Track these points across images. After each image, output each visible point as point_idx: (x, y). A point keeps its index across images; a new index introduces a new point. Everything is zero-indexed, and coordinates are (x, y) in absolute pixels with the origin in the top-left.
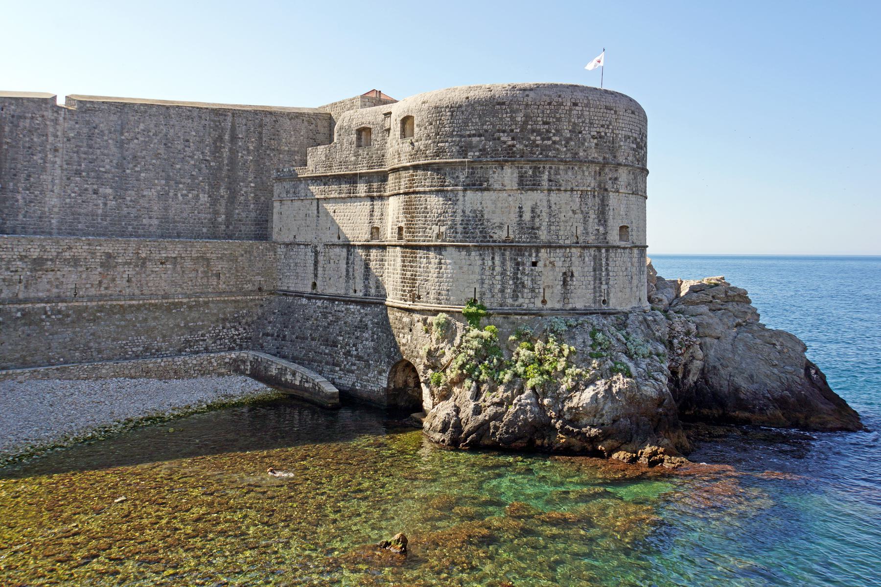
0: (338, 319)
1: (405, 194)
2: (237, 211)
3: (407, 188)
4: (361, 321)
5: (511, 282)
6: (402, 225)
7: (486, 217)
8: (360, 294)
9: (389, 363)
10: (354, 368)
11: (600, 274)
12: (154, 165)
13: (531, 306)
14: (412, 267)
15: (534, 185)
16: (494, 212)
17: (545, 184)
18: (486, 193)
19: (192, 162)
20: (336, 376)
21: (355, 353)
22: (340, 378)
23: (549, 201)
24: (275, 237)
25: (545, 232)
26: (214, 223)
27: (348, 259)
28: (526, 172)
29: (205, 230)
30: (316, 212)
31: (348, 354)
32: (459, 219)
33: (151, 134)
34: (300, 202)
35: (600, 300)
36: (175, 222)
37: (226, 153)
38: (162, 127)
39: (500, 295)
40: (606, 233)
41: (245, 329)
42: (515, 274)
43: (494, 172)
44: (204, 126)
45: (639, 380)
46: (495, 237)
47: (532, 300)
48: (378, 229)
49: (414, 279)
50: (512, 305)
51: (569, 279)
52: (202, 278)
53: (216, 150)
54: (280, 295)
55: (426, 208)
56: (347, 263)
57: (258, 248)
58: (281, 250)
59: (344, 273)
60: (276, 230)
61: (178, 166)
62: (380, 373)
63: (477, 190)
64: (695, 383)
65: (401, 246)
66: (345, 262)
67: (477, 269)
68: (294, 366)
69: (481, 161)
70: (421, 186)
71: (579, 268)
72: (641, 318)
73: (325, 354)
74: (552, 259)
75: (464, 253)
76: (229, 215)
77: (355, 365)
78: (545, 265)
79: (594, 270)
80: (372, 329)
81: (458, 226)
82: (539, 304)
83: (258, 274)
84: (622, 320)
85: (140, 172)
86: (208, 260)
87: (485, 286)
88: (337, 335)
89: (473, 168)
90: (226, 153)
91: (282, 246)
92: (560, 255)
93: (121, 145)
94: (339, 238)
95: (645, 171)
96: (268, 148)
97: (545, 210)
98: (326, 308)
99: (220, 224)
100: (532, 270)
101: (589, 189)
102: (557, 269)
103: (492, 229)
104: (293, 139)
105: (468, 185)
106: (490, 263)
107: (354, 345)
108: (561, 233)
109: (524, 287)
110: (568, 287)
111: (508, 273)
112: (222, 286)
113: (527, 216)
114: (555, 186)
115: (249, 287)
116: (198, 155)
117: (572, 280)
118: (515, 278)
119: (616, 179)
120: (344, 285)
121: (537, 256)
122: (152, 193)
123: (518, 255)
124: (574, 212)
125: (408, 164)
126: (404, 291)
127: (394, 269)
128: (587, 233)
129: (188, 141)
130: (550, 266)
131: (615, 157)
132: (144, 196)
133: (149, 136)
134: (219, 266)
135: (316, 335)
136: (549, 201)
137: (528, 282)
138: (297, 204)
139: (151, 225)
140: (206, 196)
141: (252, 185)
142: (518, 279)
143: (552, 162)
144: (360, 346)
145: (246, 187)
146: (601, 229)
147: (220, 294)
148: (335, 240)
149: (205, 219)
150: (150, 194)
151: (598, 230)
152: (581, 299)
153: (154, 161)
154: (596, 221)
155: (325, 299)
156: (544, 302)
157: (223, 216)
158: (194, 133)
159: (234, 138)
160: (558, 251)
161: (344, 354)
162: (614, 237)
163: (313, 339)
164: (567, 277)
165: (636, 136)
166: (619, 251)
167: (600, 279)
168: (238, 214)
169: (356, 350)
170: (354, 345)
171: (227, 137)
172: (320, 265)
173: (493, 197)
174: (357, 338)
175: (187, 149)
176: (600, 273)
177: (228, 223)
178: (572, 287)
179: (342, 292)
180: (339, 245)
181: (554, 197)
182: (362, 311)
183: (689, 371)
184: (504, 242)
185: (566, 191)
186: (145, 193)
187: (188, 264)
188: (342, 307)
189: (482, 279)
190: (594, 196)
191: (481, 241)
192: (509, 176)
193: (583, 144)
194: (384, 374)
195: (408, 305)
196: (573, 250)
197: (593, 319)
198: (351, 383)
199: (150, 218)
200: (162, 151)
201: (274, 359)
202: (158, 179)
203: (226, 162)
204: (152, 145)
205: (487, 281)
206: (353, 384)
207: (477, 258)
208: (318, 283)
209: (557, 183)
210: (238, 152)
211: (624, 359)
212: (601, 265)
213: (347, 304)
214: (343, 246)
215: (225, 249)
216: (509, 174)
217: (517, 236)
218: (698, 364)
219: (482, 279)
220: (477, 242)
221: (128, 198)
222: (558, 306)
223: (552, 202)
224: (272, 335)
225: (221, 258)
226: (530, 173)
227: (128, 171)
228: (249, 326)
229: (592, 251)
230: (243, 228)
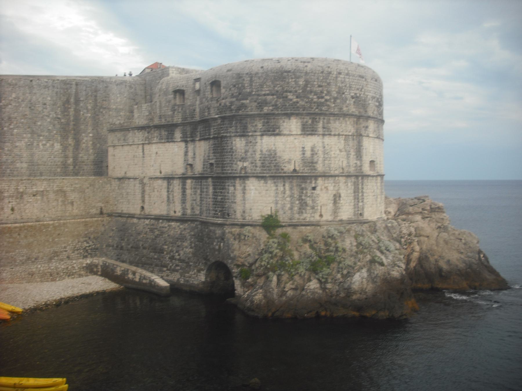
0: (162, 233)
1: (214, 138)
2: (81, 155)
3: (215, 134)
4: (181, 234)
5: (297, 202)
6: (212, 161)
7: (278, 155)
8: (179, 214)
9: (206, 263)
10: (178, 268)
11: (358, 195)
12: (22, 123)
13: (312, 219)
14: (221, 192)
15: (313, 131)
16: (284, 151)
17: (320, 130)
18: (278, 137)
19: (49, 120)
20: (164, 274)
21: (178, 257)
22: (168, 276)
23: (323, 142)
24: (110, 173)
25: (321, 165)
26: (65, 165)
27: (168, 188)
28: (307, 122)
29: (59, 170)
30: (141, 154)
31: (172, 258)
32: (258, 156)
33: (20, 100)
34: (128, 147)
35: (358, 213)
36: (38, 165)
37: (72, 111)
38: (27, 95)
39: (289, 212)
40: (361, 166)
41: (93, 242)
42: (300, 196)
43: (284, 122)
44: (57, 93)
45: (389, 267)
46: (286, 169)
47: (313, 215)
48: (191, 165)
49: (223, 202)
50: (298, 219)
51: (337, 199)
52: (61, 205)
53: (65, 110)
54: (116, 216)
55: (232, 149)
56: (168, 191)
57: (99, 182)
58: (115, 183)
59: (166, 199)
60: (110, 168)
61: (39, 123)
62: (199, 271)
63: (271, 135)
64: (414, 267)
65: (212, 177)
66: (166, 190)
67: (273, 193)
68: (134, 268)
69: (274, 114)
70: (227, 133)
71: (345, 191)
72: (384, 225)
73: (155, 259)
74: (326, 185)
75: (262, 182)
76: (75, 158)
77: (177, 265)
78: (321, 190)
79: (354, 192)
80: (190, 240)
81: (258, 162)
82: (317, 217)
83: (100, 201)
84: (373, 227)
85: (13, 129)
86: (64, 192)
87: (279, 205)
88: (163, 245)
89: (267, 119)
90: (72, 111)
91: (116, 180)
92: (332, 181)
94: (161, 173)
95: (382, 121)
96: (101, 107)
97: (321, 149)
98: (153, 225)
99: (69, 165)
100: (312, 193)
101: (350, 134)
102: (330, 192)
103: (283, 163)
104: (119, 100)
105: (264, 131)
106: (282, 189)
107: (177, 252)
108: (332, 166)
109: (307, 205)
110: (337, 205)
111: (295, 196)
112: (76, 212)
113: (308, 154)
114: (327, 132)
115: (94, 211)
116: (53, 115)
117: (339, 200)
118: (300, 199)
119: (367, 127)
120: (166, 208)
121: (315, 183)
122: (22, 144)
123: (302, 182)
124: (341, 151)
125: (217, 116)
126: (216, 211)
127: (206, 195)
128: (349, 166)
129: (45, 104)
130: (324, 191)
131: (366, 111)
132: (16, 147)
133: (18, 102)
134: (73, 196)
135: (147, 245)
136: (323, 142)
137: (309, 201)
138: (126, 148)
139: (22, 168)
140: (59, 144)
141: (91, 135)
142: (302, 200)
143: (325, 115)
144: (182, 253)
145: (87, 137)
146: (358, 162)
147: (74, 217)
148: (158, 174)
149: (59, 162)
150: (21, 144)
151: (356, 163)
152: (346, 212)
153: (22, 120)
154: (355, 157)
155: (152, 219)
156: (321, 216)
157: (71, 159)
158: (49, 98)
159: (77, 101)
160: (330, 179)
161: (169, 258)
162: (366, 169)
163: (144, 248)
164: (337, 198)
165: (378, 96)
166: (370, 178)
167: (358, 199)
168: (82, 157)
169: (179, 255)
170: (177, 252)
171: (72, 100)
172: (147, 193)
173: (283, 140)
174: (178, 246)
175: (45, 110)
176: (358, 195)
177: (75, 164)
178: (340, 205)
179: (164, 213)
180: (161, 178)
181: (327, 140)
182: (181, 226)
183: (411, 260)
184: (292, 173)
185: (335, 135)
186: (17, 144)
187: (52, 196)
188: (166, 224)
189: (276, 200)
190: (353, 139)
191: (276, 173)
193: (346, 102)
194: (202, 272)
195: (220, 221)
196: (340, 178)
197: (355, 227)
198: (176, 279)
199: (22, 162)
200: (27, 113)
201: (118, 263)
202: (25, 133)
203: (72, 118)
204: (21, 109)
205: (280, 202)
206: (178, 280)
207: (272, 185)
208: (146, 207)
209: (329, 129)
210: (80, 111)
211: (378, 254)
212: (358, 188)
213: (169, 222)
214: (164, 178)
215: (76, 184)
216: (294, 124)
217: (302, 169)
218: (416, 255)
219: (276, 200)
220: (272, 173)
221: (6, 149)
222: (330, 218)
223: (326, 143)
224: (113, 246)
225: (74, 190)
226: (310, 122)
227: (5, 129)
228: (96, 239)
229: (353, 179)
230: (85, 167)
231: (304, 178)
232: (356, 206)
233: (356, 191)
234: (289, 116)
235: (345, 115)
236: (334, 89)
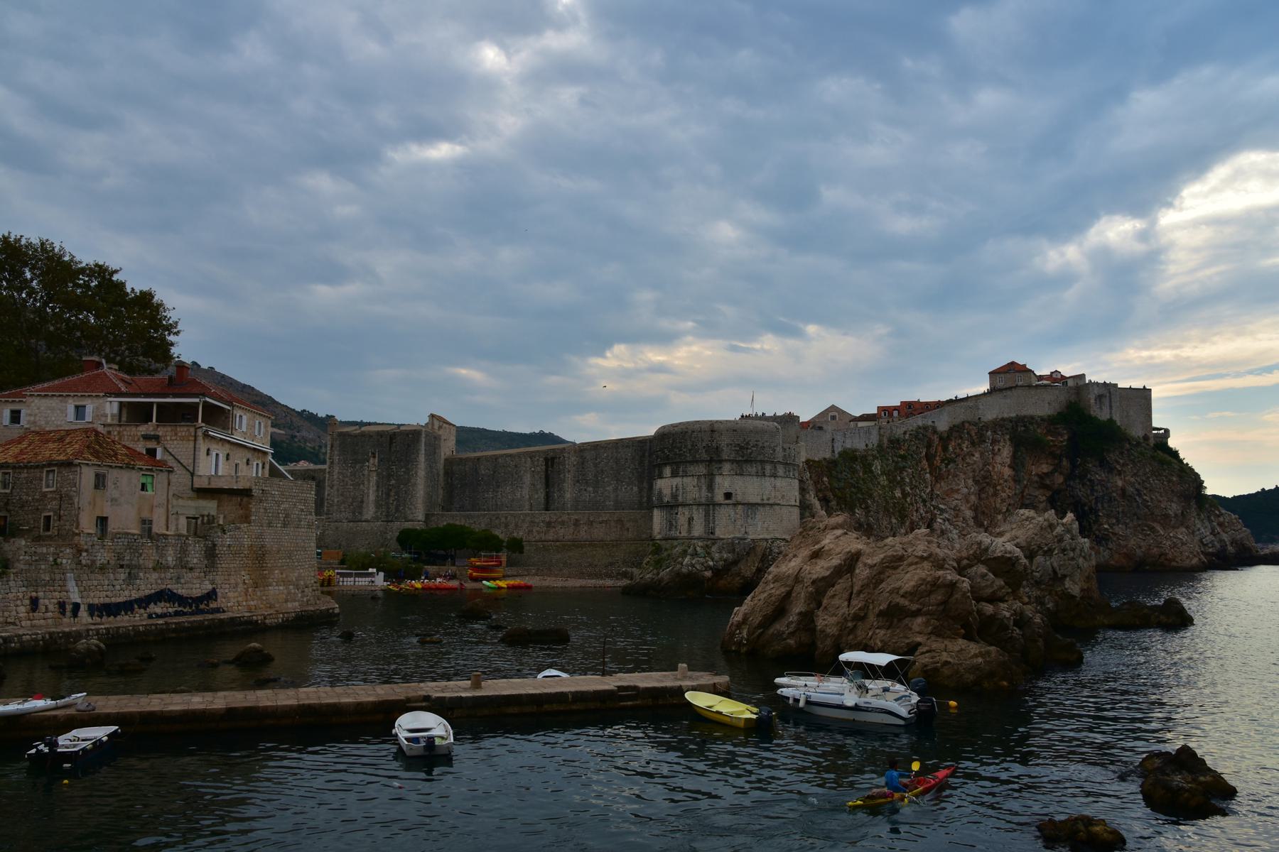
93: (596, 465)
114: (685, 475)
122: (610, 488)
134: (628, 525)
162: (719, 498)
164: (691, 520)
187: (613, 524)
192: (667, 471)
231: (671, 507)
232: (707, 525)
233: (707, 515)
234: (665, 464)
235: (697, 462)
236: (689, 443)
